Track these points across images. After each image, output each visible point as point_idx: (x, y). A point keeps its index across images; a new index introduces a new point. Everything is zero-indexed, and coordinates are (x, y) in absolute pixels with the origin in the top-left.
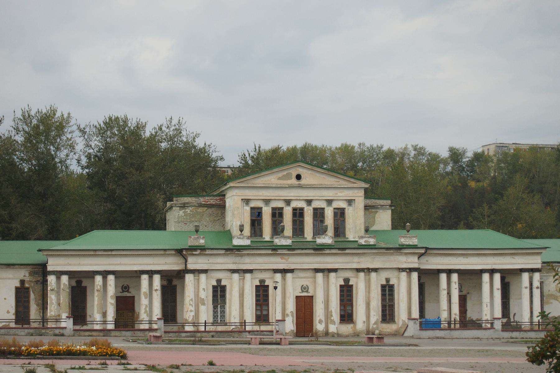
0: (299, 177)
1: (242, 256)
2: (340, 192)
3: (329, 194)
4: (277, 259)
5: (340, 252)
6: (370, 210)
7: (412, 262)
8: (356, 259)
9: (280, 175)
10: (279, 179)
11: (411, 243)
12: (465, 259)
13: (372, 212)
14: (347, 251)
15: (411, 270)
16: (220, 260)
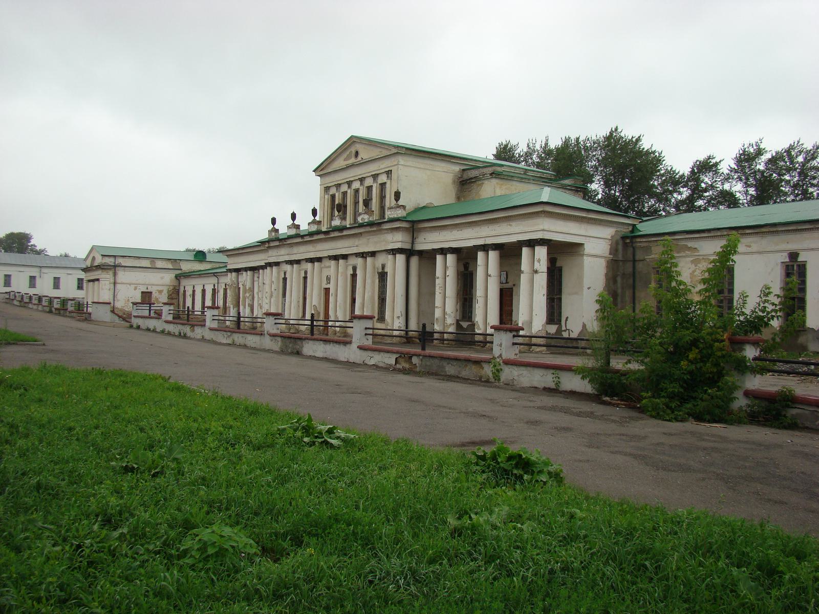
0: (357, 154)
1: (291, 245)
2: (382, 164)
3: (373, 168)
4: (309, 248)
5: (340, 234)
6: (477, 182)
7: (398, 240)
8: (356, 241)
9: (345, 156)
10: (345, 160)
11: (396, 216)
12: (460, 232)
13: (479, 185)
14: (345, 233)
15: (394, 252)
16: (283, 251)
